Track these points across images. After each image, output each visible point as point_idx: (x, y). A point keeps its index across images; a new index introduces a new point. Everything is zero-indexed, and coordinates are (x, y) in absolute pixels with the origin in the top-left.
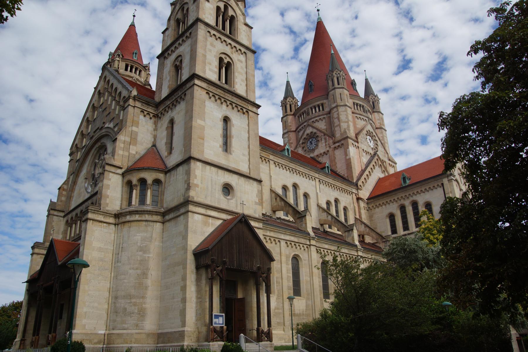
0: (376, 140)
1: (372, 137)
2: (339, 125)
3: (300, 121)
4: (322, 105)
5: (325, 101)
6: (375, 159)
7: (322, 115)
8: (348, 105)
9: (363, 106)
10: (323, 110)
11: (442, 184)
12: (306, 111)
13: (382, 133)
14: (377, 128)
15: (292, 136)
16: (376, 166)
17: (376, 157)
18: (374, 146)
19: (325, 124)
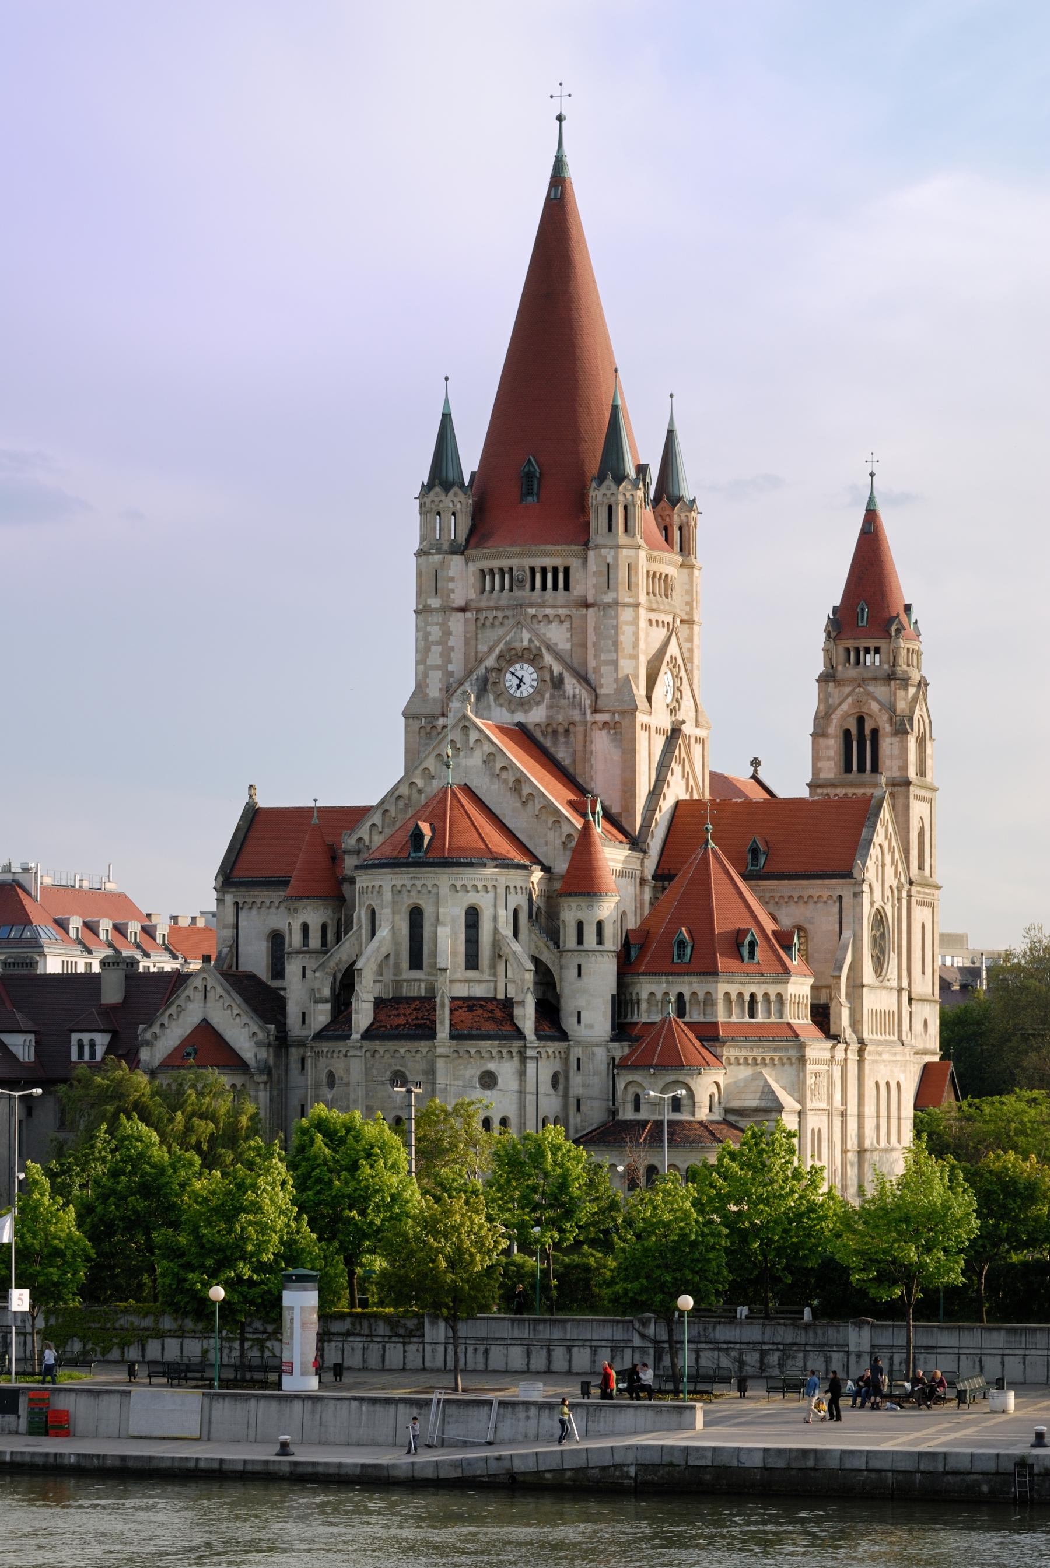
2: (615, 663)
3: (488, 588)
4: (567, 570)
7: (562, 607)
10: (567, 588)
11: (840, 897)
12: (515, 573)
19: (569, 635)
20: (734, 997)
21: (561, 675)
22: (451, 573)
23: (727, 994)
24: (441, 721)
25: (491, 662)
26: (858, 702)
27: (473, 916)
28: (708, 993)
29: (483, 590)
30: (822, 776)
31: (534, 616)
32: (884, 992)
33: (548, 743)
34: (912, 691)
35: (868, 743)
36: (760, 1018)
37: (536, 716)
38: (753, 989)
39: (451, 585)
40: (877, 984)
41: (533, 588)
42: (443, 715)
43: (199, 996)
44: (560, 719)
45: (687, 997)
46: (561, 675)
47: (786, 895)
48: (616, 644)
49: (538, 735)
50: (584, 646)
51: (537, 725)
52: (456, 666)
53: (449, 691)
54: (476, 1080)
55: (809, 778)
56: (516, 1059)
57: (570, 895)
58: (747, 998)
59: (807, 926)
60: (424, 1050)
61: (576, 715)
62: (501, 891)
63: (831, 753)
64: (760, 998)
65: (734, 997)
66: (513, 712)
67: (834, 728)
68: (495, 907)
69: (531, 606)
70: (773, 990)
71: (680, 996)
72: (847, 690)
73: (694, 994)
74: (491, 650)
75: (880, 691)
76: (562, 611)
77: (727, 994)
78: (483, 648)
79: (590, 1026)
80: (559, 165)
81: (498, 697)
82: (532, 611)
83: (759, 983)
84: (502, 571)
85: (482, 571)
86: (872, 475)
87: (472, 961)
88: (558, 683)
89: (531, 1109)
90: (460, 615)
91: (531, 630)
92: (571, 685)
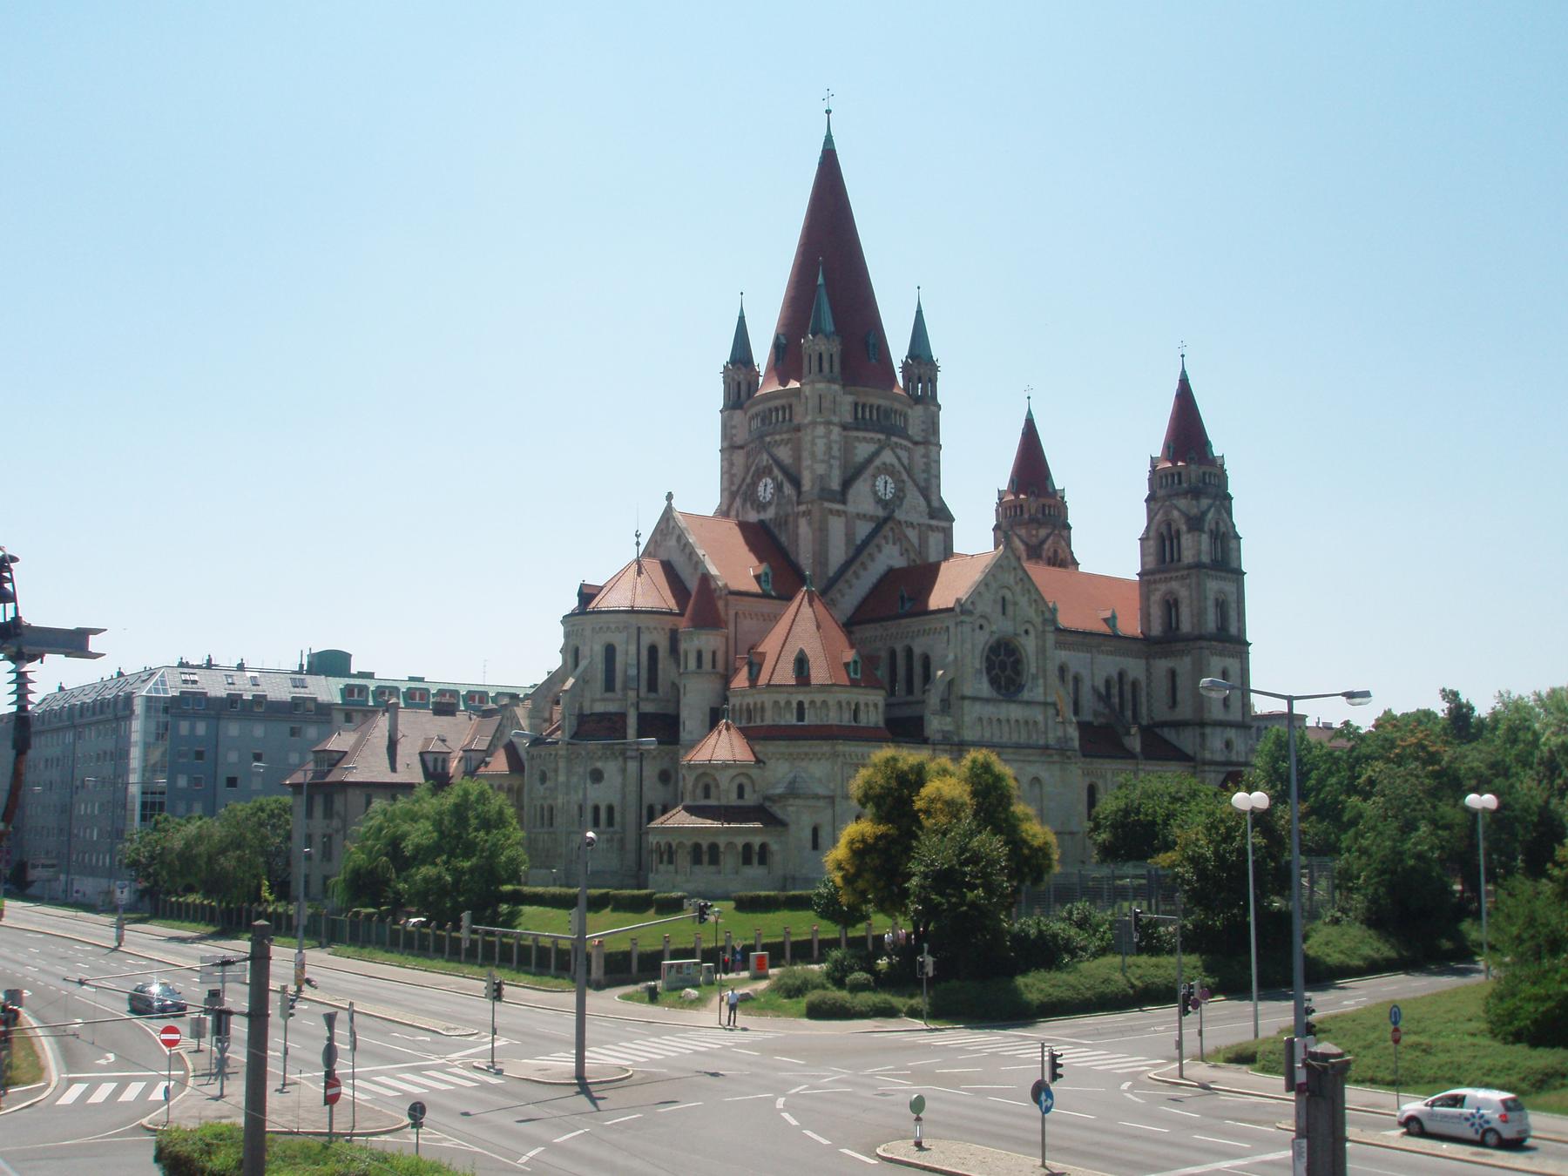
0: (903, 481)
1: (891, 475)
4: (790, 406)
5: (794, 401)
6: (886, 530)
7: (786, 432)
8: (836, 419)
9: (879, 407)
10: (790, 420)
11: (948, 628)
13: (926, 456)
14: (916, 443)
15: (739, 458)
16: (887, 543)
17: (890, 524)
18: (894, 495)
19: (790, 453)
20: (782, 703)
22: (733, 423)
23: (776, 703)
25: (748, 480)
26: (1167, 513)
27: (610, 651)
28: (763, 703)
30: (1147, 567)
31: (769, 443)
32: (1013, 707)
33: (776, 531)
34: (1205, 502)
35: (1175, 541)
36: (806, 722)
37: (769, 514)
38: (800, 697)
39: (734, 431)
40: (1001, 698)
41: (771, 423)
43: (509, 722)
44: (781, 513)
45: (751, 707)
47: (916, 630)
48: (813, 455)
49: (772, 526)
50: (798, 458)
51: (771, 520)
52: (734, 488)
54: (588, 775)
55: (1139, 570)
56: (620, 759)
58: (794, 705)
59: (932, 655)
60: (553, 753)
61: (789, 509)
62: (636, 632)
63: (1152, 550)
64: (806, 706)
65: (782, 703)
67: (1152, 534)
68: (627, 643)
69: (767, 436)
70: (819, 698)
71: (748, 704)
72: (1159, 504)
73: (755, 704)
75: (1182, 503)
76: (785, 436)
77: (776, 703)
79: (690, 733)
80: (829, 140)
81: (752, 505)
82: (768, 439)
83: (805, 692)
86: (1183, 356)
87: (609, 685)
89: (632, 798)
90: (741, 451)
92: (788, 489)
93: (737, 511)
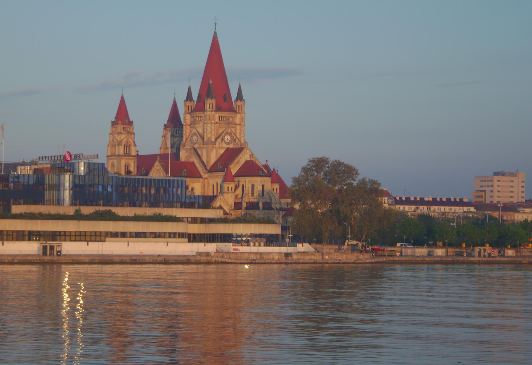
3: (221, 119)
21: (235, 138)
24: (215, 146)
29: (220, 120)
42: (215, 145)
46: (235, 138)
53: (216, 139)
57: (227, 181)
66: (227, 145)
74: (223, 132)
78: (220, 132)
82: (230, 125)
84: (224, 117)
85: (220, 116)
88: (235, 140)
91: (230, 129)
93: (219, 143)
